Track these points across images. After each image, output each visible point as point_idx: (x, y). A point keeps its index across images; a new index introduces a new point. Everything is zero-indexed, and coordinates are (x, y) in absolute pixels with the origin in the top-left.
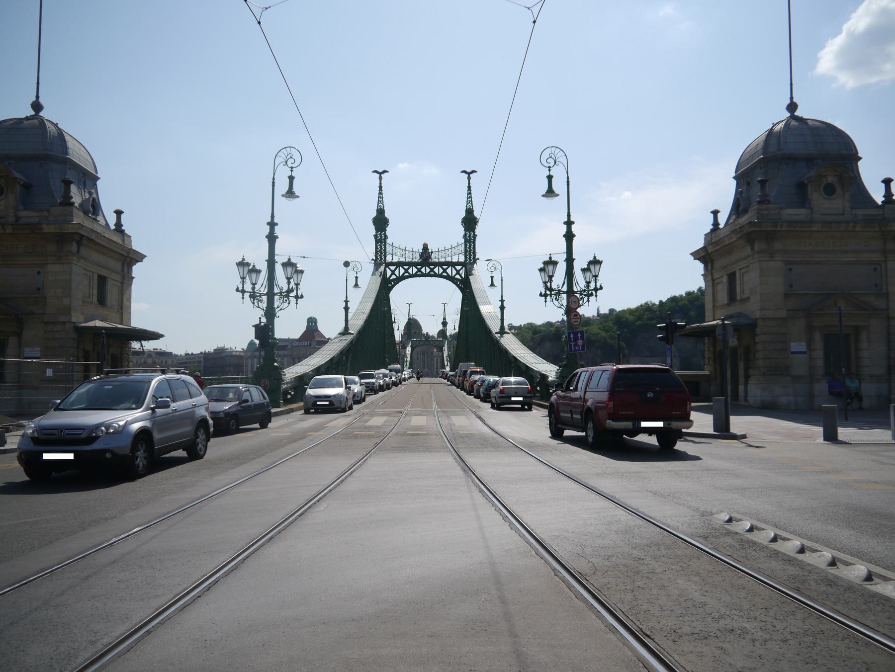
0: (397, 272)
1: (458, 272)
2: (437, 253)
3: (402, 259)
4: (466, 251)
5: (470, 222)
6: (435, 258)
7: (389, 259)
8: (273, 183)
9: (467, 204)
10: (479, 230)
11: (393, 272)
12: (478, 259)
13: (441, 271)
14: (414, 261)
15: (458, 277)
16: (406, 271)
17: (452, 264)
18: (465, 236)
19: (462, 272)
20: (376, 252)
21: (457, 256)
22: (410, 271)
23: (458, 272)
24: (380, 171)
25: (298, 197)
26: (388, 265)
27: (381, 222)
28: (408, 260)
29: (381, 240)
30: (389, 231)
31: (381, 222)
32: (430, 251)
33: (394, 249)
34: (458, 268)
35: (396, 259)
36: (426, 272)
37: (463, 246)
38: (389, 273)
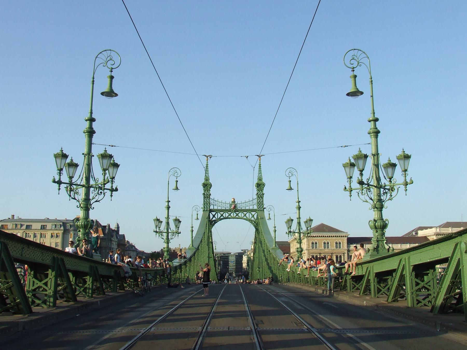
0: (216, 216)
3: (219, 208)
4: (258, 203)
5: (260, 186)
6: (239, 207)
9: (259, 174)
10: (266, 190)
11: (214, 216)
12: (265, 208)
13: (243, 215)
14: (227, 209)
15: (253, 219)
16: (222, 215)
18: (257, 194)
19: (255, 217)
20: (204, 204)
22: (224, 215)
23: (253, 216)
26: (211, 211)
27: (207, 186)
28: (223, 208)
29: (207, 196)
30: (212, 191)
31: (207, 186)
32: (236, 203)
34: (253, 213)
35: (216, 208)
36: (234, 215)
37: (256, 200)
38: (211, 216)
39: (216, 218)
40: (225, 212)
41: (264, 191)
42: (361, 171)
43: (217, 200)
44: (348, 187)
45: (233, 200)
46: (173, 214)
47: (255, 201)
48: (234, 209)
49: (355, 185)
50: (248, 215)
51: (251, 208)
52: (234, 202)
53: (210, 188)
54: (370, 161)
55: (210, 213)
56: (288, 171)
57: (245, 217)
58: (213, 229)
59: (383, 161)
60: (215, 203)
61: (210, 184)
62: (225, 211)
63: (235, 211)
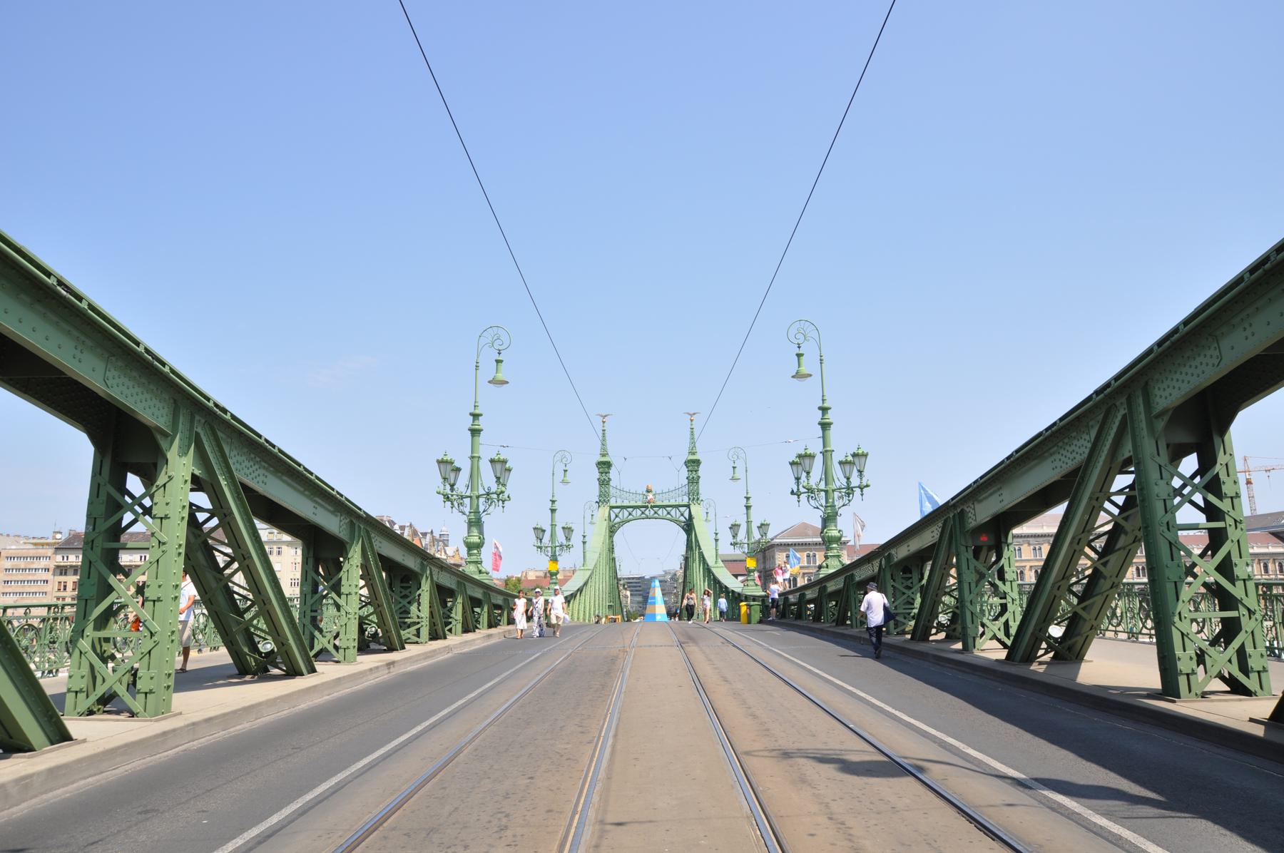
0: (621, 515)
1: (682, 515)
3: (626, 503)
5: (693, 464)
13: (665, 512)
15: (682, 519)
16: (630, 514)
17: (677, 507)
19: (686, 515)
21: (680, 498)
24: (604, 414)
27: (605, 466)
29: (604, 483)
30: (613, 473)
31: (605, 466)
33: (618, 491)
34: (682, 509)
38: (613, 516)
41: (700, 473)
42: (808, 473)
44: (795, 490)
46: (561, 521)
47: (685, 489)
49: (802, 490)
54: (818, 462)
56: (731, 452)
58: (617, 537)
59: (837, 457)
63: (652, 507)
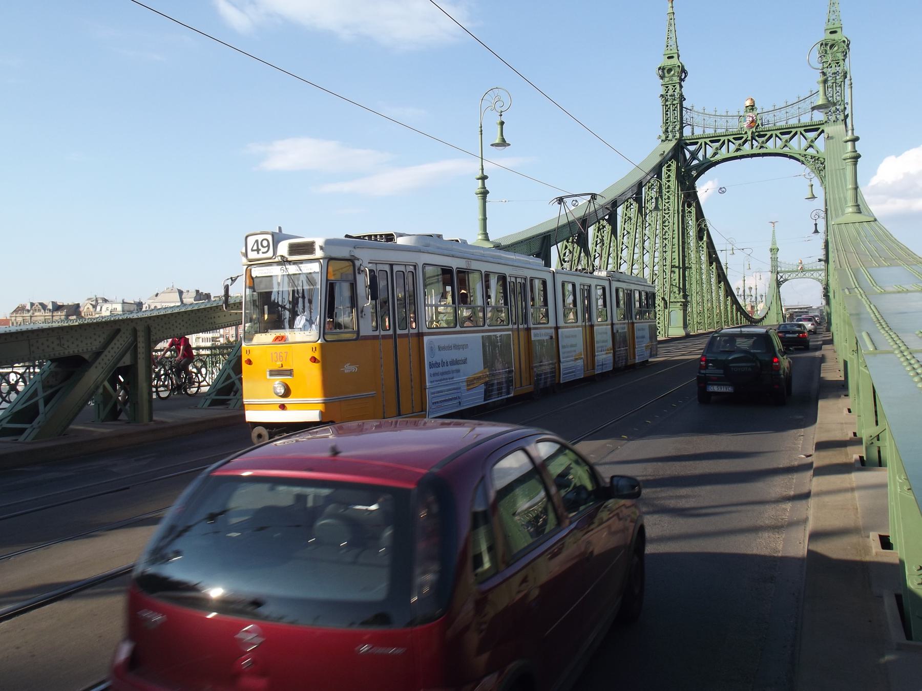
0: (700, 155)
2: (771, 115)
3: (710, 132)
7: (687, 132)
8: (481, 131)
11: (694, 155)
25: (509, 145)
38: (688, 155)
39: (699, 160)
40: (724, 143)
43: (703, 111)
45: (748, 103)
48: (752, 127)
50: (797, 144)
51: (806, 120)
52: (752, 107)
53: (683, 80)
55: (685, 150)
57: (786, 150)
60: (698, 119)
61: (679, 66)
62: (726, 138)
